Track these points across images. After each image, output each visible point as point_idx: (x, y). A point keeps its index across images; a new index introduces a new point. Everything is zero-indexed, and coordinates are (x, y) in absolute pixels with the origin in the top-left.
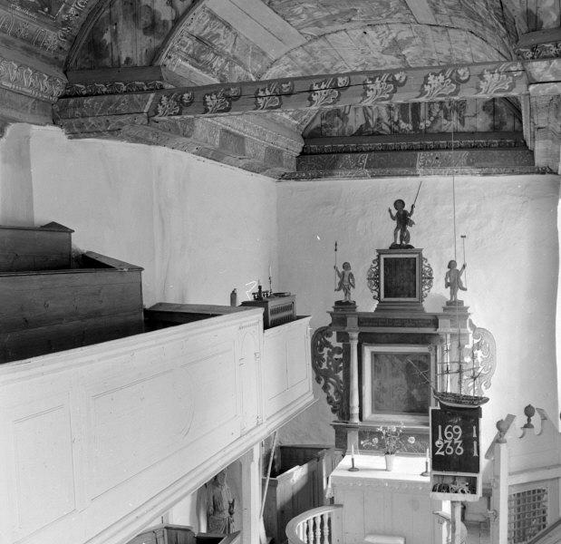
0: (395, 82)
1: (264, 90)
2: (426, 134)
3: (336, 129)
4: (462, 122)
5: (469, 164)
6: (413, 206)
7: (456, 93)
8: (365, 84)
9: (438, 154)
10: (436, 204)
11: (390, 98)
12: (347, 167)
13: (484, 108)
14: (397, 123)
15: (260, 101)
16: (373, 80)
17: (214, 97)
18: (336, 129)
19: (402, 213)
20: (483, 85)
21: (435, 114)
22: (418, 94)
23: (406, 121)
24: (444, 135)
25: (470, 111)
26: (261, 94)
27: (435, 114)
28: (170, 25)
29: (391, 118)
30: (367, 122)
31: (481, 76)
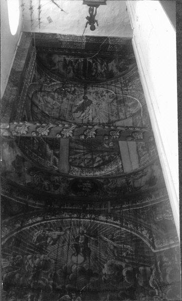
0: (61, 135)
1: (116, 138)
2: (81, 56)
3: (122, 62)
4: (65, 60)
5: (61, 42)
6: (86, 27)
7: (38, 127)
8: (73, 136)
9: (75, 48)
10: (78, 21)
11: (63, 129)
12: (118, 46)
13: (55, 64)
14: (93, 62)
15: (118, 134)
16: (69, 136)
17: (139, 138)
18: (122, 62)
19: (92, 24)
20: (26, 129)
21: (77, 64)
22: (52, 129)
23: (89, 62)
24: (74, 55)
25: (61, 64)
26: (117, 137)
27: (77, 64)
28: (155, 164)
29: (96, 64)
30: (107, 64)
31: (27, 132)
